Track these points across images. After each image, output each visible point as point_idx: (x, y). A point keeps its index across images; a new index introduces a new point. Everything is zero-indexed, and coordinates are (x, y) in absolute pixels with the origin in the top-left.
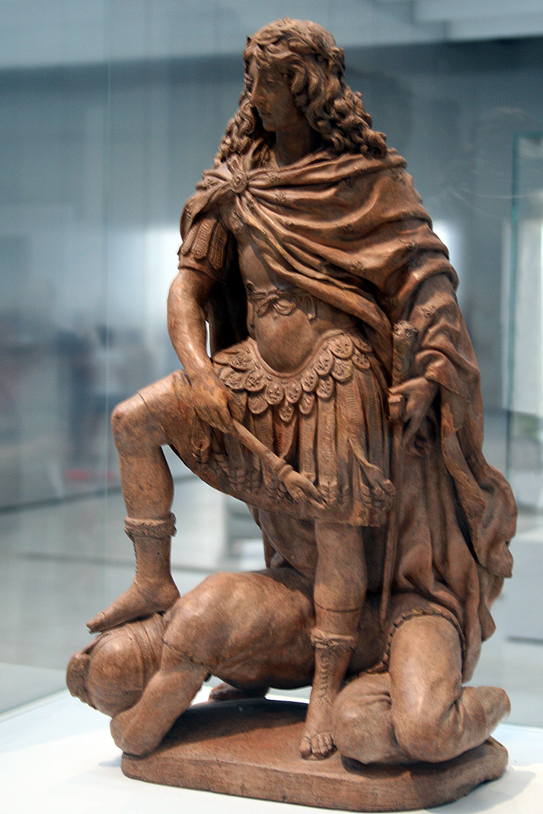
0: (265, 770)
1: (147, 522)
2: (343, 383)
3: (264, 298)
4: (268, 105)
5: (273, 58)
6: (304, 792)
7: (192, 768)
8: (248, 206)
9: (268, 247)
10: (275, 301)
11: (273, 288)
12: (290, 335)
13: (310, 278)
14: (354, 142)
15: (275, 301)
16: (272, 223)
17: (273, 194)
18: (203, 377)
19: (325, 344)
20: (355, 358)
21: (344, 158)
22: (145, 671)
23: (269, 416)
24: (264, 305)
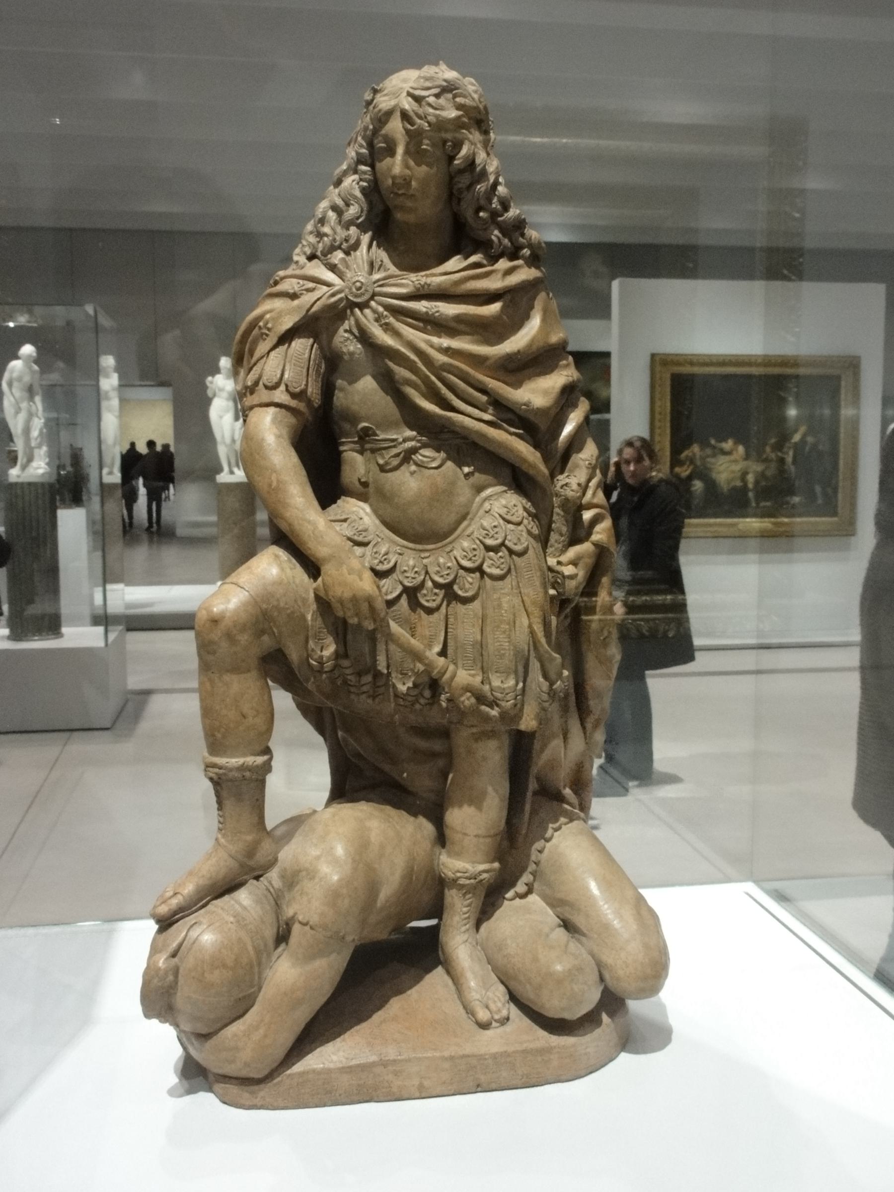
0: (452, 1058)
2: (521, 554)
3: (394, 446)
4: (413, 183)
5: (437, 116)
6: (504, 1074)
8: (377, 320)
9: (414, 378)
10: (414, 451)
12: (441, 496)
13: (472, 420)
15: (414, 451)
16: (423, 346)
17: (422, 306)
19: (487, 506)
20: (525, 521)
21: (503, 264)
22: (260, 964)
23: (404, 601)
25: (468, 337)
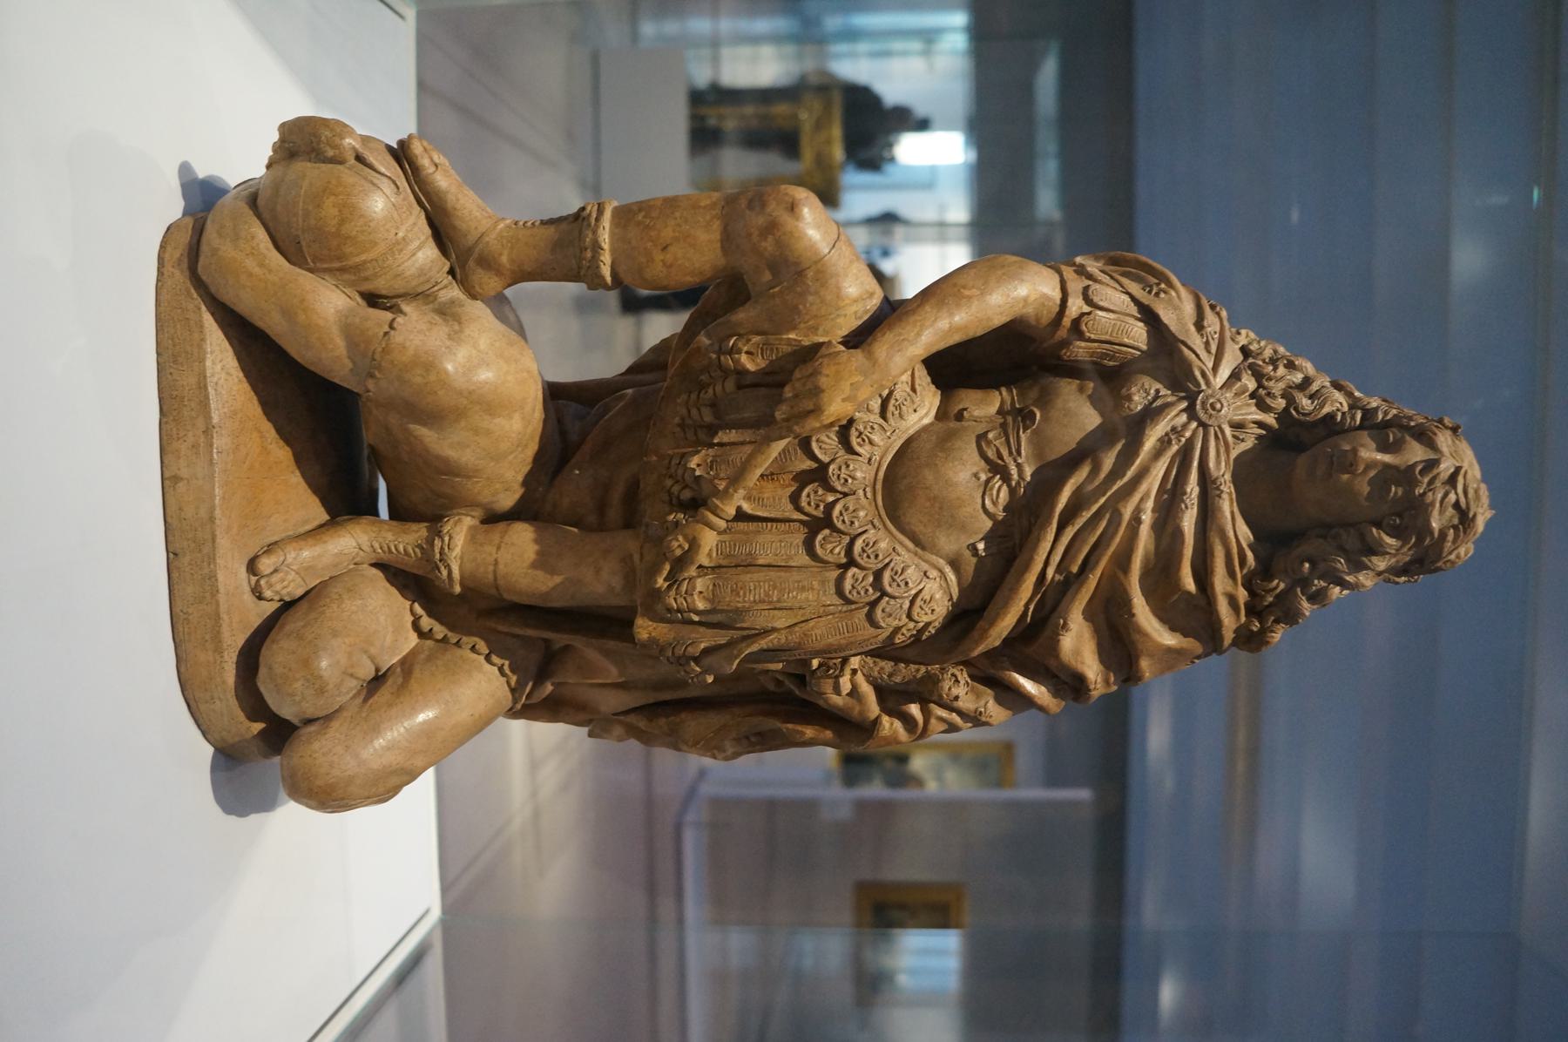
0: (212, 519)
1: (606, 258)
2: (870, 618)
3: (1011, 453)
4: (1346, 477)
5: (1432, 504)
6: (190, 590)
7: (193, 380)
8: (1174, 429)
9: (1102, 475)
10: (1006, 478)
11: (1028, 472)
12: (945, 513)
13: (1047, 553)
14: (1265, 610)
15: (1006, 478)
16: (1143, 487)
17: (1193, 487)
18: (875, 377)
19: (933, 573)
20: (911, 625)
21: (1242, 595)
22: (342, 270)
23: (808, 464)
24: (1000, 457)
25: (1152, 547)
